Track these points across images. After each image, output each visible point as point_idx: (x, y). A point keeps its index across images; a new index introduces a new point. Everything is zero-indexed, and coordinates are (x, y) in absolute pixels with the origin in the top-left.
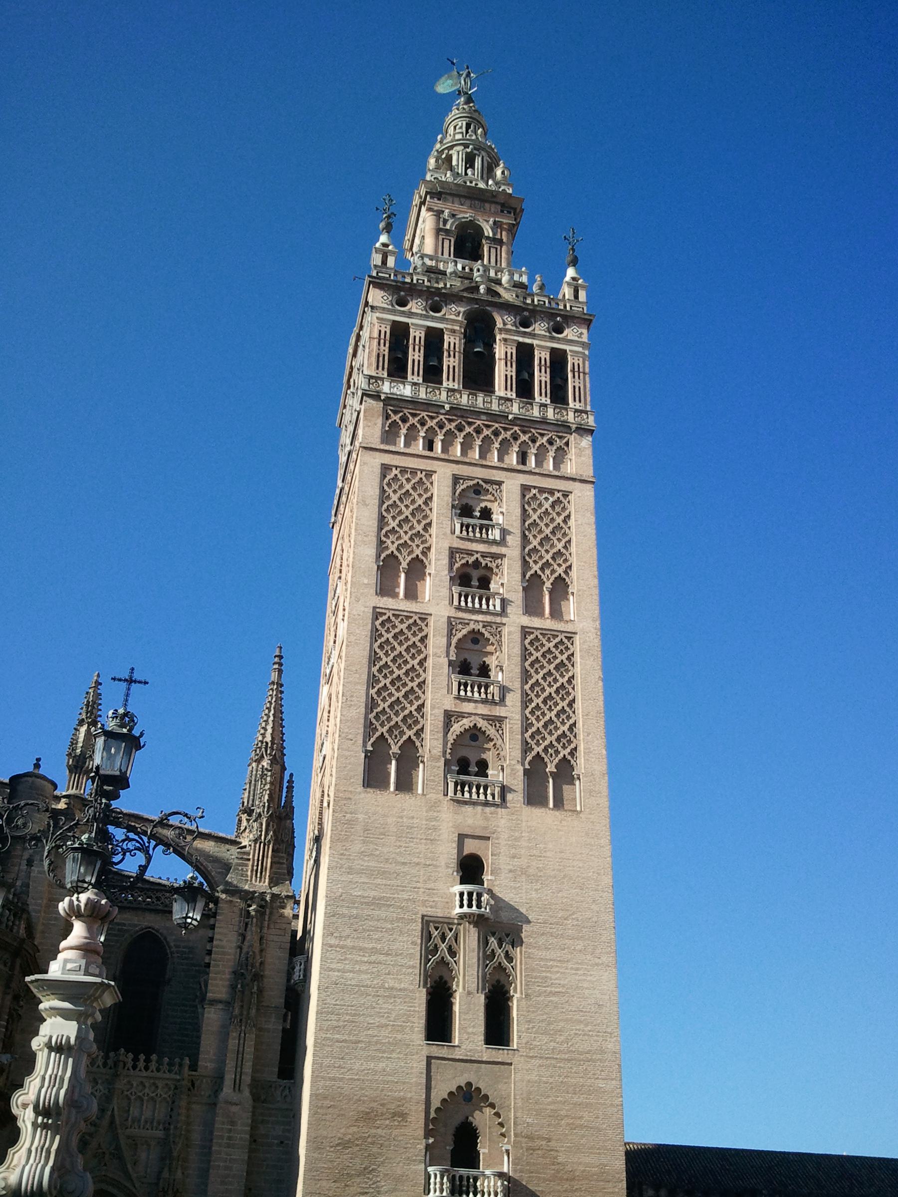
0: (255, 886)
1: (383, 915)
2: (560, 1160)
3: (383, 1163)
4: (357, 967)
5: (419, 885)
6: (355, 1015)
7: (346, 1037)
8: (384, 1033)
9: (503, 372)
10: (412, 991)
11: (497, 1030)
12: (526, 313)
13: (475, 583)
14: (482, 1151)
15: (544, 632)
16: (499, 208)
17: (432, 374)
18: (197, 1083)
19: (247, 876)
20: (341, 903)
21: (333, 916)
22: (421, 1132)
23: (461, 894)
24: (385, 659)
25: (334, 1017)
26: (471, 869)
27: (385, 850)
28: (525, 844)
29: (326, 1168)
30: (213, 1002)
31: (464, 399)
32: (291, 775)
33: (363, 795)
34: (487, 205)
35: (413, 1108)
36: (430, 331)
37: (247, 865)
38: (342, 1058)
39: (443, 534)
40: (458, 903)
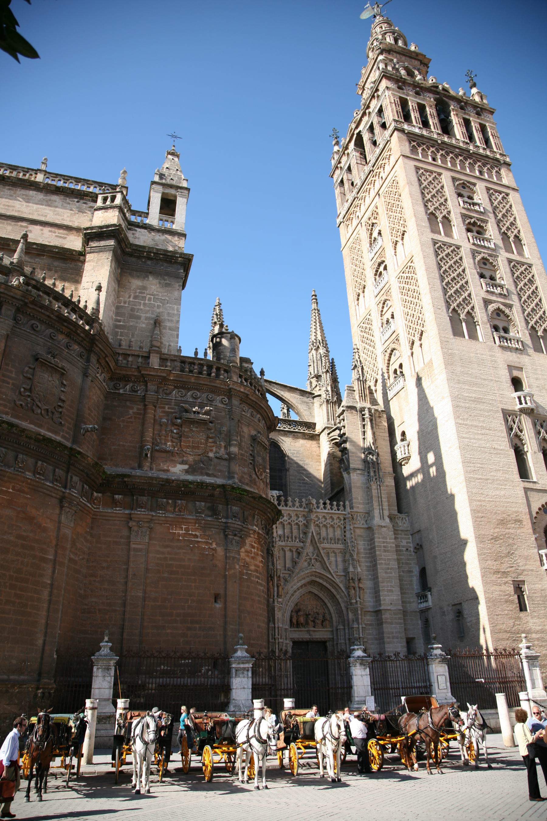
1: (482, 407)
3: (517, 549)
4: (476, 437)
5: (495, 392)
6: (482, 464)
7: (480, 477)
8: (499, 474)
10: (507, 451)
12: (463, 104)
15: (518, 262)
17: (425, 124)
18: (355, 517)
20: (459, 400)
22: (531, 531)
23: (519, 398)
26: (517, 383)
27: (474, 371)
28: (540, 373)
29: (490, 553)
30: (355, 469)
31: (446, 139)
33: (454, 340)
34: (413, 61)
35: (524, 517)
36: (419, 105)
39: (455, 207)
40: (518, 402)
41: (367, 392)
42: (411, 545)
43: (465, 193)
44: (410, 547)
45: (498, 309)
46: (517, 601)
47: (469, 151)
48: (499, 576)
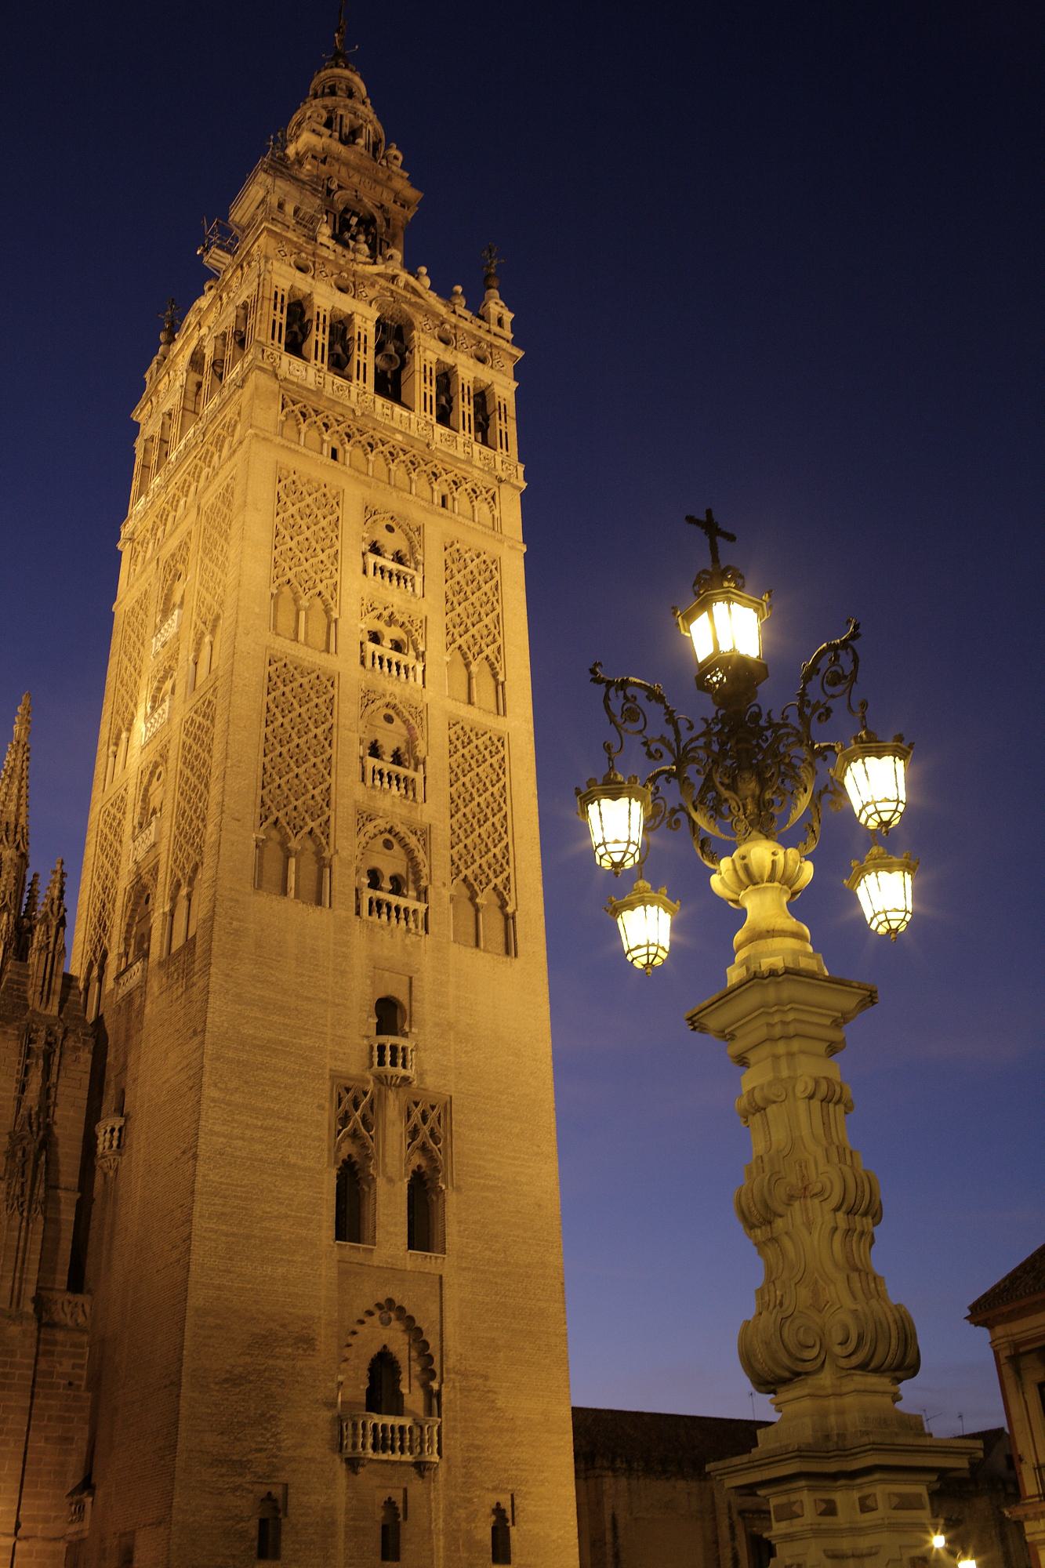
0: (40, 1015)
2: (499, 1404)
9: (421, 388)
11: (423, 1231)
13: (387, 643)
14: (405, 1390)
16: (392, 197)
19: (26, 999)
21: (218, 1059)
23: (382, 1048)
24: (281, 720)
25: (217, 1200)
32: (36, 875)
34: (379, 189)
35: (323, 1332)
37: (25, 984)
38: (230, 1259)
40: (376, 1060)
41: (58, 984)
42: (84, 1373)
43: (393, 542)
44: (80, 1378)
45: (390, 831)
46: (254, 1532)
47: (428, 445)
48: (224, 1470)
